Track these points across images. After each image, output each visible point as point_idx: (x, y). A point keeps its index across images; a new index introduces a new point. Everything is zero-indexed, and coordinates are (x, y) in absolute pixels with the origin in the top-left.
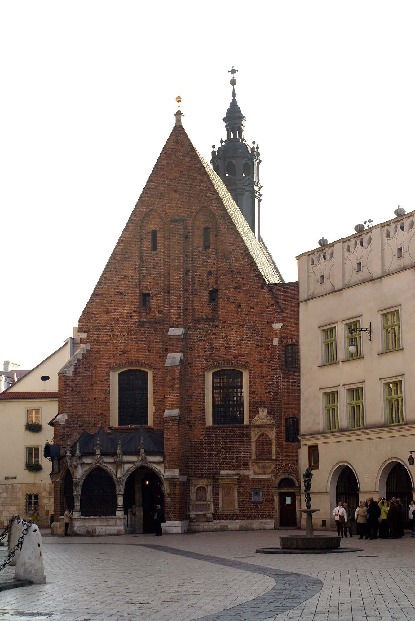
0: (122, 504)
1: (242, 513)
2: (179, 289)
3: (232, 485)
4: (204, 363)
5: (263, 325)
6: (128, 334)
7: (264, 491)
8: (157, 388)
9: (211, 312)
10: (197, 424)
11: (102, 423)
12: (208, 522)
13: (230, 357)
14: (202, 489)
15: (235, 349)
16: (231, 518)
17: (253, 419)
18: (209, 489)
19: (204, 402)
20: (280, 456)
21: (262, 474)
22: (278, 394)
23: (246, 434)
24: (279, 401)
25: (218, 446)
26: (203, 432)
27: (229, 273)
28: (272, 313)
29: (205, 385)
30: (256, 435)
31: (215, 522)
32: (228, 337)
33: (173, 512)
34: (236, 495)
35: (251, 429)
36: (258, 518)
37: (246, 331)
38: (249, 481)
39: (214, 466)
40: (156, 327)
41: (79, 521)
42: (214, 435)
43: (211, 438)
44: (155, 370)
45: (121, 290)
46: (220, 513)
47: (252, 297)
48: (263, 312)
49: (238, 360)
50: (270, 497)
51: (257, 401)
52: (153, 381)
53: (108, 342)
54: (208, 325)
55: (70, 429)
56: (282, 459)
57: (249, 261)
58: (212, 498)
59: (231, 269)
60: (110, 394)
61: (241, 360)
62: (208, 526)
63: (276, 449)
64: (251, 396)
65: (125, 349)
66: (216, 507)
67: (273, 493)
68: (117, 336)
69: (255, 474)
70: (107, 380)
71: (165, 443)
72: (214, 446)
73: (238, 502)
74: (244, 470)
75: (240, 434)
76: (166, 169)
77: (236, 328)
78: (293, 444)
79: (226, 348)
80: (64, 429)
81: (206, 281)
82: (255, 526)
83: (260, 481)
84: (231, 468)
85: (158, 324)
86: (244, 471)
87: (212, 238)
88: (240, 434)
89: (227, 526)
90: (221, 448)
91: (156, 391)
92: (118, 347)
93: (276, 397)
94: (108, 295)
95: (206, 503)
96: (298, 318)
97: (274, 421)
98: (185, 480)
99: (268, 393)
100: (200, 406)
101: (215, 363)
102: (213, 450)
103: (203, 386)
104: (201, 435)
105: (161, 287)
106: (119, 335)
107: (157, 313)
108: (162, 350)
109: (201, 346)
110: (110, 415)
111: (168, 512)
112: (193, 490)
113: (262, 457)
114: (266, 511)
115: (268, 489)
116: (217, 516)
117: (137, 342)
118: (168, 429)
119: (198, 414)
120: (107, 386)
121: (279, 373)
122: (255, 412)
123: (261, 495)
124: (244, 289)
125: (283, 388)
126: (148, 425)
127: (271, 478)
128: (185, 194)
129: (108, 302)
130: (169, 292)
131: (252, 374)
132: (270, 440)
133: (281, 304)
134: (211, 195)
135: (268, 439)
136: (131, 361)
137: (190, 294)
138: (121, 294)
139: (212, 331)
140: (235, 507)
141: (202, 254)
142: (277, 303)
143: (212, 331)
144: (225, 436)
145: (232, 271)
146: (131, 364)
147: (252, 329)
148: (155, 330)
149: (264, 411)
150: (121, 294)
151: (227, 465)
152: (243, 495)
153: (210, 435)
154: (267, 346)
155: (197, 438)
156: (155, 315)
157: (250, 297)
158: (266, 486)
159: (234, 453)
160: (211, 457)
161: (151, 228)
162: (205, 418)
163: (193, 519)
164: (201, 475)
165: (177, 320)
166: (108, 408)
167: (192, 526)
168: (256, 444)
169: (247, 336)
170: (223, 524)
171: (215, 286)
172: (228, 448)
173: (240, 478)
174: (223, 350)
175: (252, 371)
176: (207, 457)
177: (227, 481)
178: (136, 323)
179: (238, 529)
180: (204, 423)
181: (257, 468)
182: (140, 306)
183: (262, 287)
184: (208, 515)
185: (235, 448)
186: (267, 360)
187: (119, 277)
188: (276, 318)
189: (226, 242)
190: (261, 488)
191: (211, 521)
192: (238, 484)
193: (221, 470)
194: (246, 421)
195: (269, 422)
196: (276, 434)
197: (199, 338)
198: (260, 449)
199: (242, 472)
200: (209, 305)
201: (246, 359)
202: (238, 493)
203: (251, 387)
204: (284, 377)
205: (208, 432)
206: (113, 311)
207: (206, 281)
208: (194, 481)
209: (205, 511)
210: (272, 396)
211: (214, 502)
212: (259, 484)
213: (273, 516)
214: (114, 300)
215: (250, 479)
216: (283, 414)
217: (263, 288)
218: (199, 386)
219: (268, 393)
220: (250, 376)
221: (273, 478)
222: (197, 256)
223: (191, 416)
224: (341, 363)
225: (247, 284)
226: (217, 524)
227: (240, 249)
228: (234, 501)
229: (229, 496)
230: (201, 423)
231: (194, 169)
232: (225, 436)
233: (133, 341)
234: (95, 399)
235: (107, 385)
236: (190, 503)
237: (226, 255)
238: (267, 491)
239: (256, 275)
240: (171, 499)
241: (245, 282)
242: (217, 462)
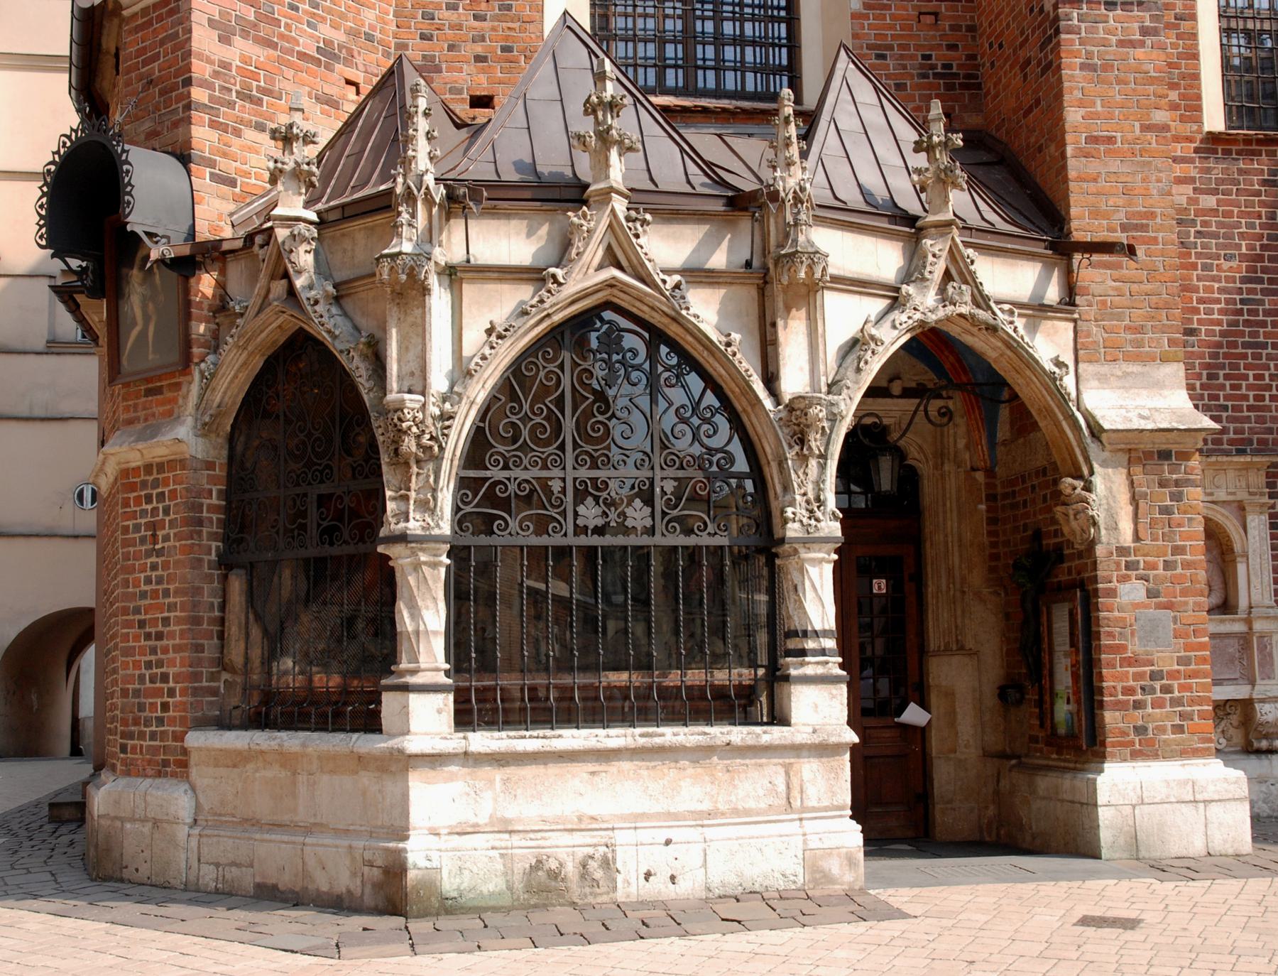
0: (831, 624)
11: (479, 59)
33: (1167, 689)
41: (452, 778)
55: (259, 54)
71: (1072, 174)
80: (225, 39)
95: (1239, 627)
102: (1261, 281)
111: (1129, 691)
118: (1092, 68)
160: (1247, 323)
184: (1267, 707)
240: (1151, 594)
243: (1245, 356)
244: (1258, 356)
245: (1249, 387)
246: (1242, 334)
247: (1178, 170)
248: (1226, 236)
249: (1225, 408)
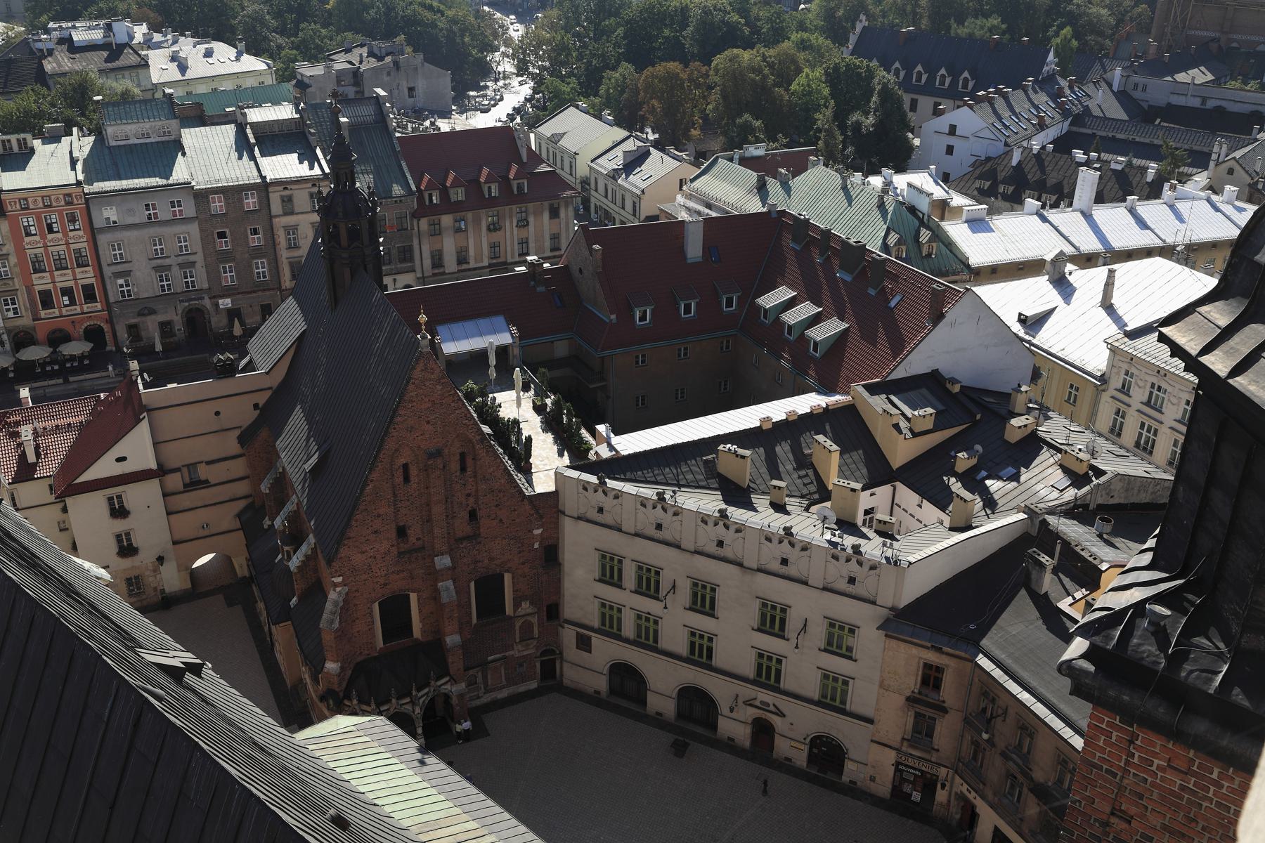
34: (503, 672)
87: (469, 462)
117: (398, 573)
126: (412, 636)
135: (531, 625)
138: (376, 532)
150: (376, 532)
174: (486, 561)
183: (523, 500)
194: (509, 610)
199: (507, 654)
201: (509, 565)
224: (628, 591)
234: (358, 632)
241: (506, 498)
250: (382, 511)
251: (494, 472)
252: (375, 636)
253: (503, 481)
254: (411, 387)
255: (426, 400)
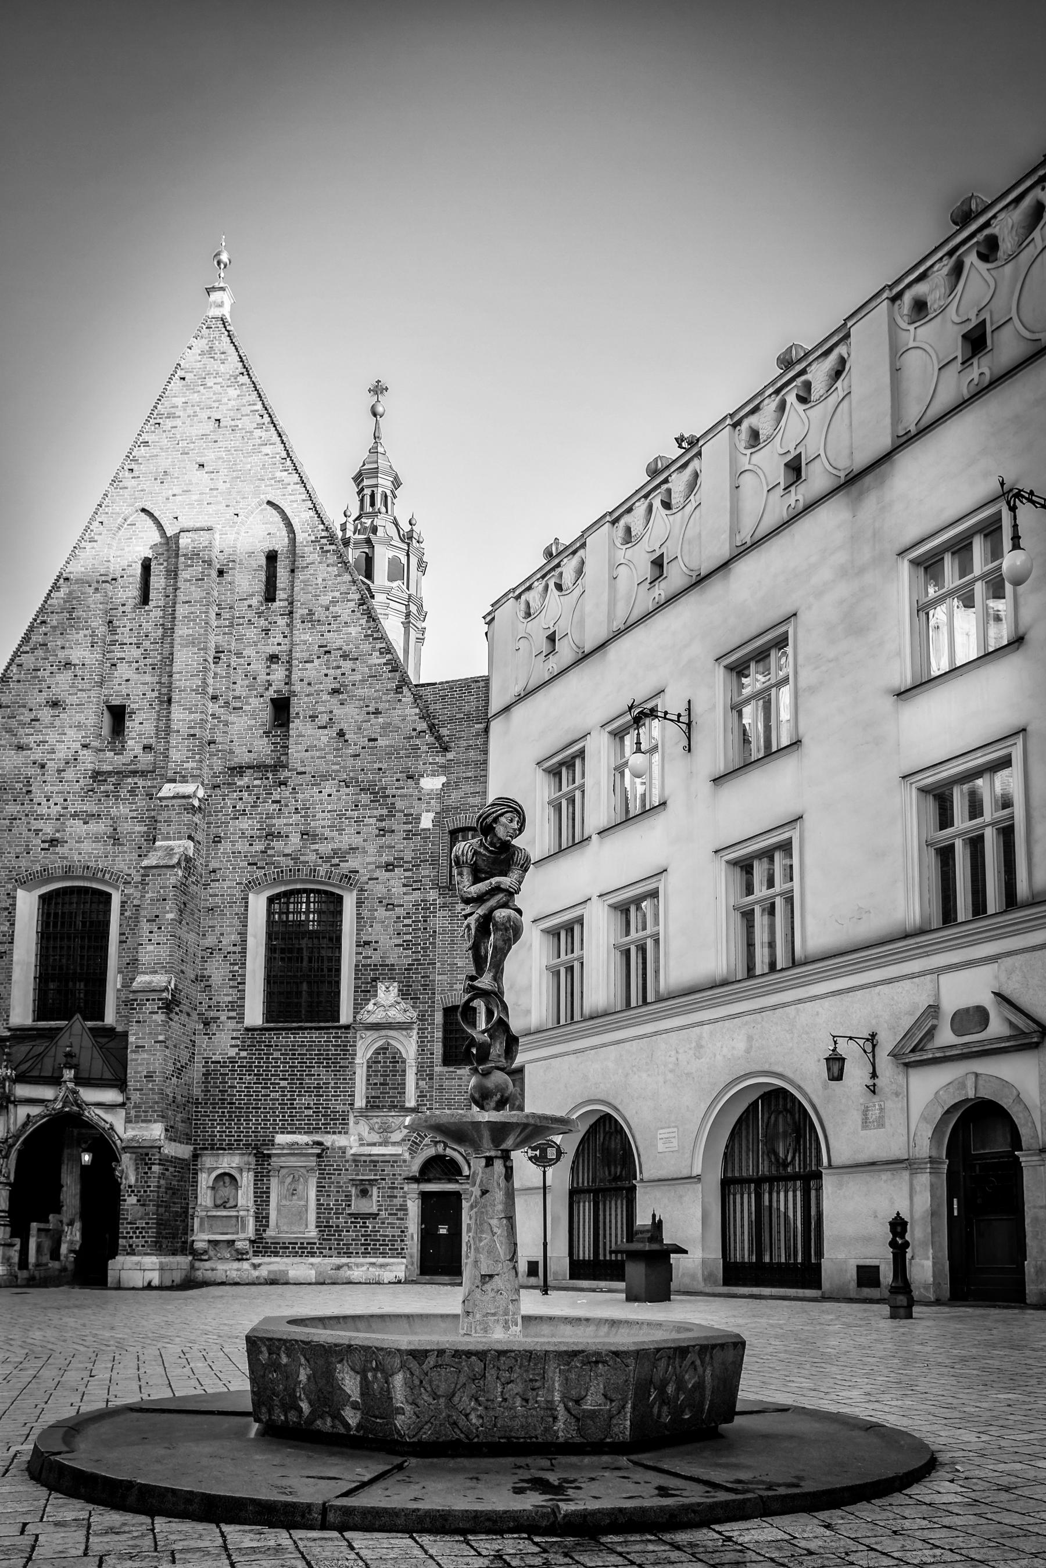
1: (324, 1240)
2: (194, 690)
3: (302, 1170)
4: (248, 872)
5: (398, 780)
6: (65, 800)
7: (383, 1188)
8: (130, 930)
9: (272, 751)
10: (223, 1018)
12: (239, 1260)
13: (312, 857)
14: (228, 1178)
15: (326, 839)
16: (297, 1252)
17: (361, 1009)
18: (245, 1179)
19: (243, 965)
20: (427, 1101)
21: (380, 1144)
22: (428, 948)
23: (344, 1046)
24: (428, 964)
25: (272, 1075)
26: (239, 1038)
27: (319, 657)
28: (423, 753)
29: (247, 926)
30: (367, 1049)
31: (256, 1260)
32: (309, 808)
35: (356, 1033)
36: (366, 1254)
37: (356, 794)
38: (347, 1161)
39: (260, 1124)
40: (136, 783)
42: (265, 1046)
43: (255, 1054)
44: (127, 886)
45: (53, 695)
46: (269, 1241)
47: (373, 713)
48: (400, 750)
49: (331, 865)
50: (398, 1201)
51: (375, 965)
52: (122, 914)
53: (15, 819)
54: (262, 779)
56: (432, 1109)
57: (369, 628)
58: (251, 1203)
59: (326, 646)
60: (12, 943)
61: (339, 865)
62: (238, 1270)
63: (417, 1084)
64: (361, 953)
65: (57, 835)
66: (260, 1226)
67: (404, 1193)
68: (39, 804)
69: (362, 1145)
70: (8, 909)
72: (262, 1075)
73: (318, 1213)
74: (334, 1133)
75: (326, 1046)
76: (181, 414)
77: (329, 787)
78: (459, 1072)
79: (303, 835)
81: (262, 677)
82: (356, 1273)
83: (374, 1162)
84: (304, 1128)
85: (140, 776)
86: (335, 1137)
88: (326, 1046)
89: (286, 1272)
90: (280, 1079)
91: (127, 938)
92: (41, 830)
93: (422, 956)
94: (25, 707)
95: (235, 1214)
96: (485, 762)
97: (415, 1014)
98: (186, 1157)
99: (403, 945)
100: (233, 976)
101: (274, 872)
102: (261, 1083)
103: (243, 926)
104: (232, 1046)
105: (153, 690)
106: (44, 802)
107: (138, 750)
108: (145, 840)
109: (242, 830)
110: (10, 995)
112: (205, 1180)
113: (380, 1102)
114: (387, 1236)
115: (394, 1183)
116: (263, 1247)
117: (87, 818)
119: (225, 995)
120: (8, 924)
121: (433, 895)
122: (369, 991)
123: (375, 1198)
124: (353, 696)
125: (439, 934)
127: (400, 1155)
128: (224, 471)
129: (23, 724)
130: (169, 701)
131: (365, 898)
132: (404, 1062)
133: (444, 731)
134: (286, 473)
136: (68, 864)
137: (223, 707)
138: (55, 704)
139: (272, 794)
140: (309, 1226)
141: (256, 613)
142: (432, 727)
143: (272, 794)
144: (290, 1050)
145: (329, 652)
146: (68, 873)
147: (369, 789)
148: (132, 792)
149: (391, 988)
150: (55, 704)
151: (292, 1120)
152: (329, 1196)
153: (255, 1046)
154: (404, 831)
155: (220, 1054)
156: (136, 757)
157: (368, 713)
158: (388, 1175)
159: (313, 1092)
160: (254, 1100)
161: (137, 552)
162: (244, 1006)
163: (202, 1254)
164: (228, 1144)
165: (186, 765)
166: (7, 976)
167: (198, 1269)
168: (368, 1071)
169: (356, 806)
170: (273, 1268)
171: (285, 689)
172: (298, 1079)
173: (322, 1152)
174: (295, 839)
175: (366, 891)
176: (244, 1100)
177: (293, 1161)
178: (88, 774)
179: (314, 1281)
180: (239, 1018)
181: (367, 1129)
182: (101, 735)
183: (398, 690)
185: (315, 1079)
186: (402, 866)
187: (52, 666)
188: (430, 764)
189: (317, 584)
190: (377, 1180)
191: (247, 1259)
192: (320, 1170)
193: (277, 1133)
195: (400, 1018)
196: (419, 1046)
197: (239, 811)
198: (376, 1084)
199: (328, 1140)
200: (267, 733)
201: (353, 863)
202: (318, 1191)
203: (362, 930)
204: (444, 906)
205: (249, 1038)
206: (32, 745)
207: (262, 677)
208: (208, 1161)
209: (233, 1234)
210: (412, 952)
211: (256, 1213)
212: (370, 1170)
213: (403, 1249)
214: (38, 720)
215: (348, 1156)
216: (437, 997)
217: (402, 693)
218: (234, 926)
219: (403, 945)
220: (360, 903)
221: (407, 1156)
222: (244, 617)
223: (211, 999)
225: (363, 681)
226: (262, 1267)
227: (348, 601)
228: (307, 1210)
229: (295, 1197)
230: (235, 1018)
231: (247, 415)
232: (290, 1050)
233: (78, 815)
235: (9, 921)
236: (196, 1213)
237: (314, 614)
238: (389, 1188)
239: (384, 661)
241: (359, 677)
242: (269, 1113)
243: (252, 1112)
244: (257, 1112)
245: (253, 1124)
246: (252, 1104)
247: (234, 1042)
248: (249, 1067)
249: (243, 1132)
250: (77, 655)
251: (334, 602)
252: (9, 978)
253: (354, 631)
254: (176, 384)
255: (203, 415)
